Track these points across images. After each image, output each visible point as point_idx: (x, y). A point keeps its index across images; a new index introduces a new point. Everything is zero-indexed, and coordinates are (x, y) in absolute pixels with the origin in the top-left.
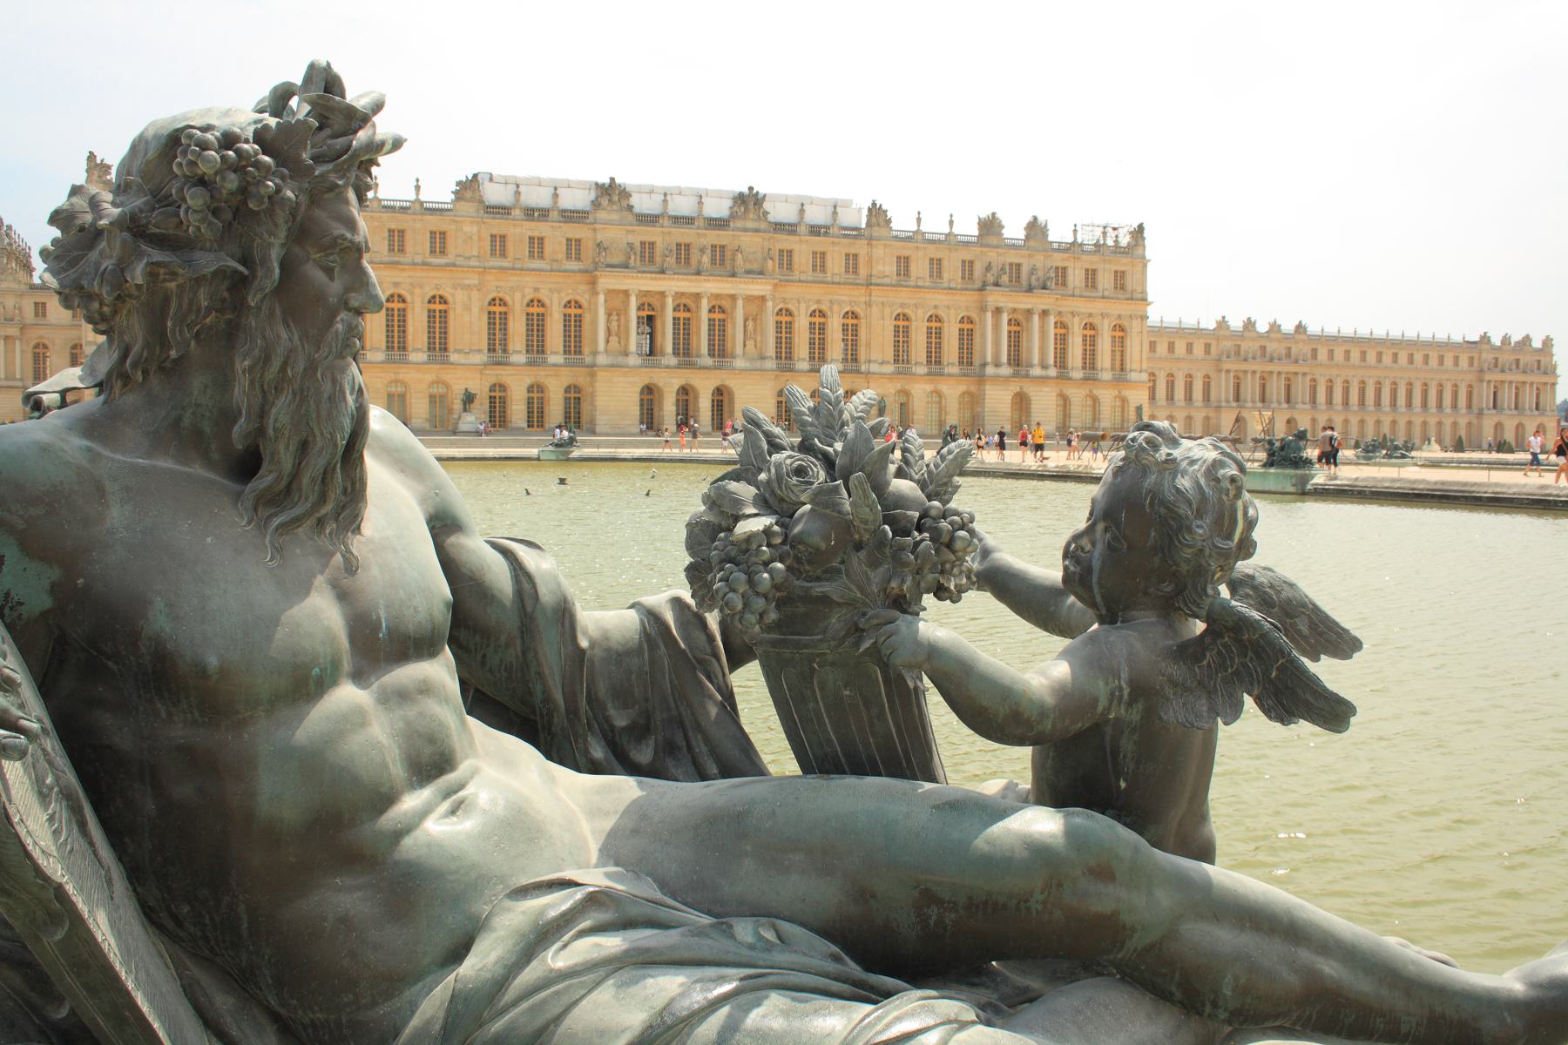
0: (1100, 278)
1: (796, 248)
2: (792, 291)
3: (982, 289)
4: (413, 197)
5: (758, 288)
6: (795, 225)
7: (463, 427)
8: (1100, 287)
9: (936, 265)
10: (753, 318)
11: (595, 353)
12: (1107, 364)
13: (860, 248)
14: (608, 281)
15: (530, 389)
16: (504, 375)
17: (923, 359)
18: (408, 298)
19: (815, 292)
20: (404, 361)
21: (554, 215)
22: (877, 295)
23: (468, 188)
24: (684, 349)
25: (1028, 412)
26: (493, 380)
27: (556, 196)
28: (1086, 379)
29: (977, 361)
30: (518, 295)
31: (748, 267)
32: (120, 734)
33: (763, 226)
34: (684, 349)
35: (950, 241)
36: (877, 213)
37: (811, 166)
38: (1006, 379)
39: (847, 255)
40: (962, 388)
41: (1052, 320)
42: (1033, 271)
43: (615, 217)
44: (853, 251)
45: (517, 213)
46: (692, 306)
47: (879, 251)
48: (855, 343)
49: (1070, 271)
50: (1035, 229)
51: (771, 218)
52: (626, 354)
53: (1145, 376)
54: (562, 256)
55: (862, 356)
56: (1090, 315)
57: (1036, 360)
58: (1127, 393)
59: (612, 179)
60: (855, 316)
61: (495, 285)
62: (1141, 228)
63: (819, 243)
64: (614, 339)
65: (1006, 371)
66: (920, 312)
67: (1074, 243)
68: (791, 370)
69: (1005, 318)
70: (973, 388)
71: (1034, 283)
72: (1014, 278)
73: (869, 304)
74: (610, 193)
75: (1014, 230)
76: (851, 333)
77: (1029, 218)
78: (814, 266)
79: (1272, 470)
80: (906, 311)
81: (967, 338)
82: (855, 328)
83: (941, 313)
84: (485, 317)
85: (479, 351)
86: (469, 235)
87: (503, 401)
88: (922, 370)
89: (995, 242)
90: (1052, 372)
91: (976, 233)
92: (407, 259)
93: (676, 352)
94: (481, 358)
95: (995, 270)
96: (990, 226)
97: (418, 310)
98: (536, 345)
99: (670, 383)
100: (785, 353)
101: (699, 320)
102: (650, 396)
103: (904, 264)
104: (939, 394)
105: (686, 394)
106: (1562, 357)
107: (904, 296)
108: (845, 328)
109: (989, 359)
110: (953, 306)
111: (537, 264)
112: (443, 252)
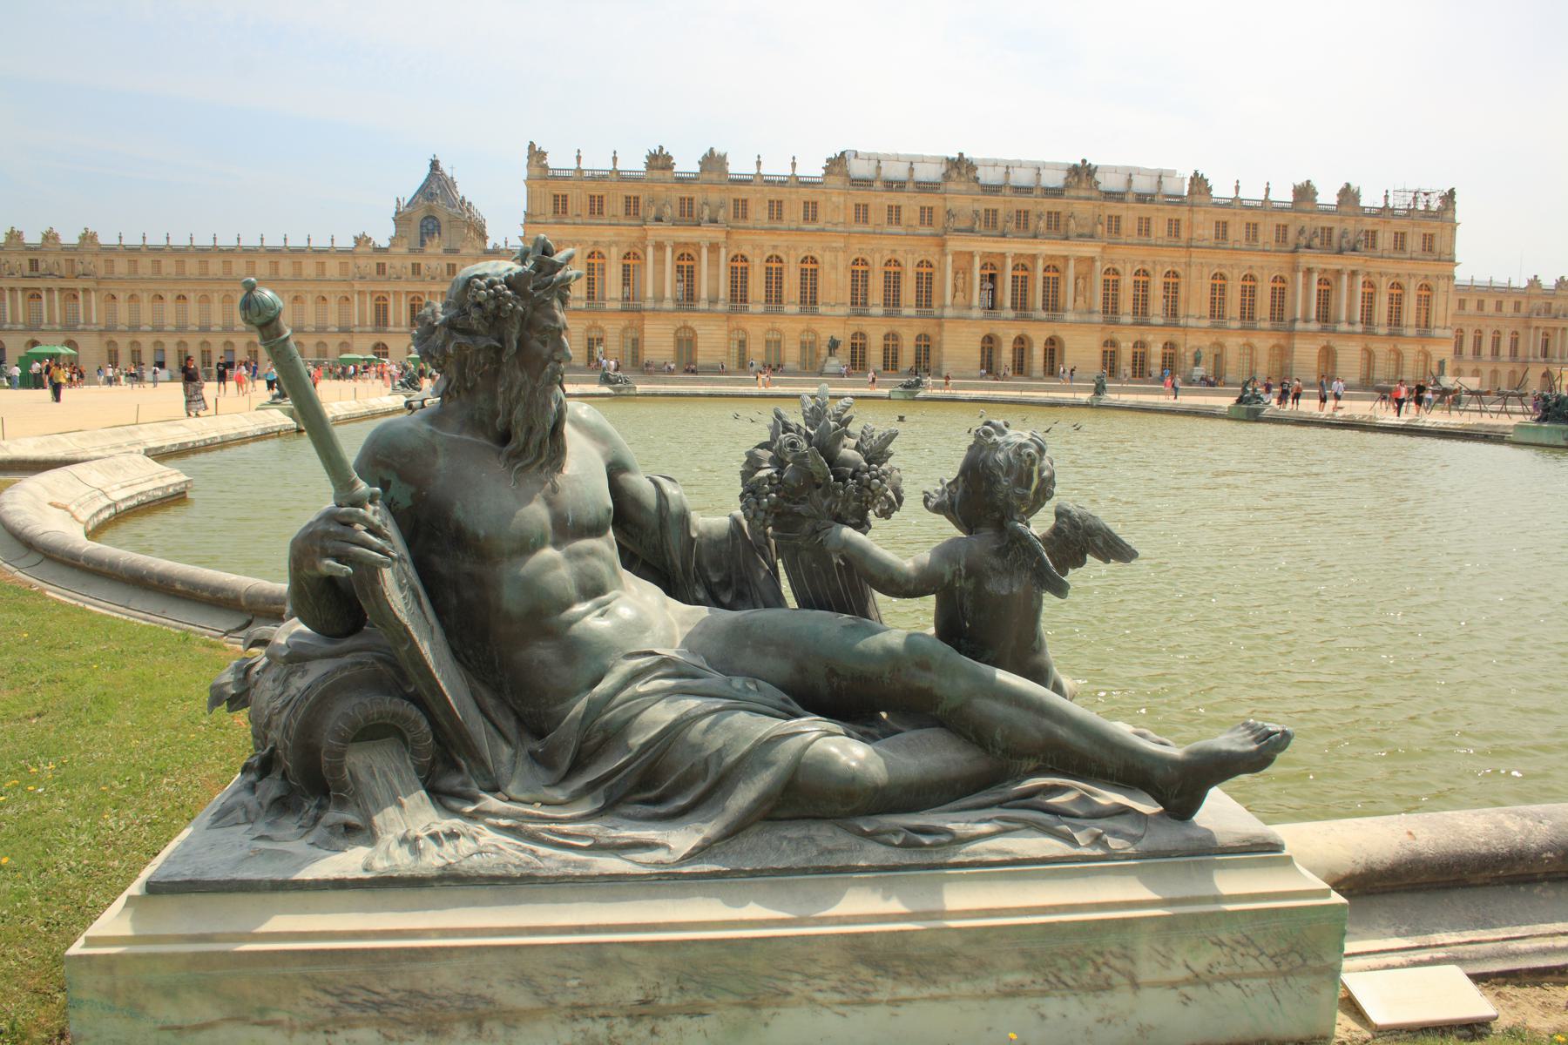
1: (1124, 214)
2: (1119, 253)
3: (1294, 251)
4: (790, 173)
5: (1088, 250)
6: (1123, 194)
7: (828, 369)
8: (1408, 249)
9: (1252, 230)
10: (1084, 277)
11: (943, 307)
12: (1412, 321)
14: (956, 244)
15: (886, 337)
16: (865, 325)
17: (1237, 314)
18: (785, 259)
19: (1140, 253)
20: (779, 312)
21: (910, 186)
22: (1197, 256)
23: (837, 164)
24: (1021, 305)
25: (1334, 365)
26: (856, 329)
27: (911, 169)
28: (1390, 335)
29: (1287, 317)
30: (877, 256)
31: (1080, 231)
32: (441, 565)
33: (1094, 194)
34: (1021, 305)
35: (1266, 207)
36: (1198, 182)
37: (1136, 141)
39: (1170, 220)
40: (1272, 342)
41: (1360, 279)
42: (1344, 234)
43: (963, 187)
44: (1175, 217)
45: (878, 185)
46: (1029, 265)
47: (1199, 217)
48: (1175, 300)
49: (1380, 234)
50: (1348, 195)
51: (1101, 187)
52: (970, 307)
53: (1448, 333)
54: (916, 222)
55: (1181, 312)
57: (1343, 317)
58: (1430, 348)
59: (961, 155)
60: (1176, 275)
61: (858, 248)
62: (1452, 193)
63: (1144, 210)
64: (959, 294)
65: (1314, 326)
66: (1236, 271)
68: (1116, 323)
69: (1315, 277)
70: (1283, 342)
71: (1344, 245)
72: (1327, 241)
73: (1188, 265)
74: (959, 166)
75: (1327, 196)
76: (1172, 290)
77: (1342, 185)
78: (1140, 230)
79: (1545, 425)
80: (1223, 271)
81: (1279, 296)
82: (1176, 286)
83: (1255, 273)
85: (844, 304)
86: (837, 206)
87: (863, 347)
88: (1236, 324)
89: (1308, 207)
90: (1359, 328)
92: (784, 225)
93: (1014, 307)
94: (844, 310)
95: (1307, 234)
96: (1304, 193)
97: (792, 269)
98: (892, 300)
99: (1007, 334)
100: (1111, 309)
101: (1035, 278)
102: (990, 343)
103: (1222, 228)
104: (1251, 347)
105: (1022, 343)
107: (1220, 259)
109: (1299, 315)
111: (894, 229)
112: (814, 219)
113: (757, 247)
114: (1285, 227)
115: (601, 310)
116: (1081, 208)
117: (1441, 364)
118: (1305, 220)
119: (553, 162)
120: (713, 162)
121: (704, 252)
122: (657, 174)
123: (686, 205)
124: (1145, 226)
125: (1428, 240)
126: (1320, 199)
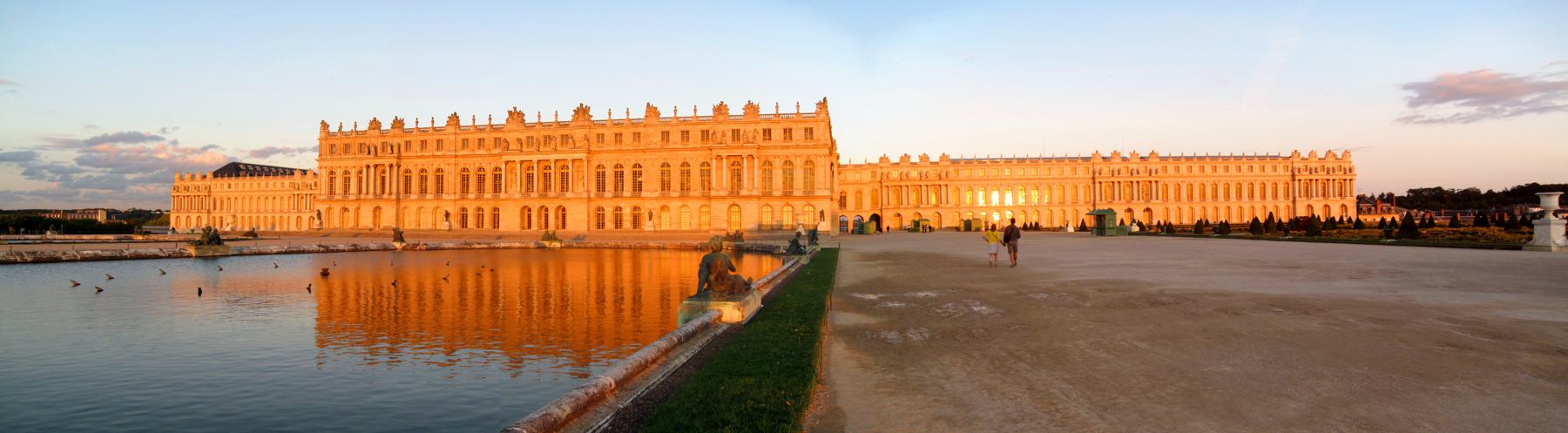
13: (641, 130)
16: (465, 204)
22: (647, 155)
36: (652, 111)
47: (651, 130)
50: (751, 108)
61: (462, 163)
67: (777, 115)
75: (736, 109)
84: (459, 179)
96: (720, 109)
99: (535, 206)
106: (1356, 161)
107: (665, 154)
108: (634, 174)
113: (413, 165)
117: (822, 213)
118: (719, 128)
119: (333, 128)
123: (736, 134)
124: (618, 136)
126: (731, 112)
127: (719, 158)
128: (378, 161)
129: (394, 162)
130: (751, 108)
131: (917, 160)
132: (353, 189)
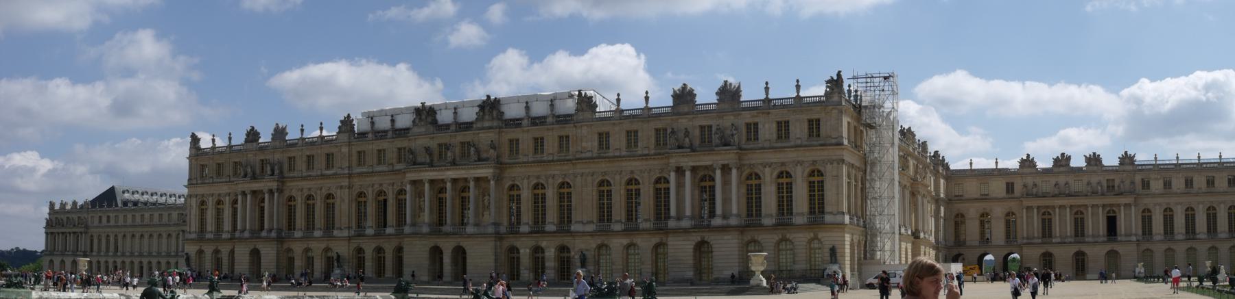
0: (791, 128)
9: (632, 137)
35: (647, 114)
38: (686, 231)
47: (585, 131)
49: (760, 126)
50: (729, 94)
56: (783, 164)
66: (617, 177)
67: (767, 101)
72: (710, 138)
75: (706, 96)
81: (661, 197)
91: (671, 104)
96: (684, 97)
103: (604, 139)
107: (603, 166)
110: (645, 171)
114: (665, 130)
115: (637, 230)
116: (485, 138)
120: (279, 133)
121: (267, 196)
122: (249, 146)
125: (814, 126)
126: (699, 100)
127: (680, 171)
128: (256, 186)
129: (274, 185)
130: (729, 94)
131: (1083, 164)
132: (227, 226)
